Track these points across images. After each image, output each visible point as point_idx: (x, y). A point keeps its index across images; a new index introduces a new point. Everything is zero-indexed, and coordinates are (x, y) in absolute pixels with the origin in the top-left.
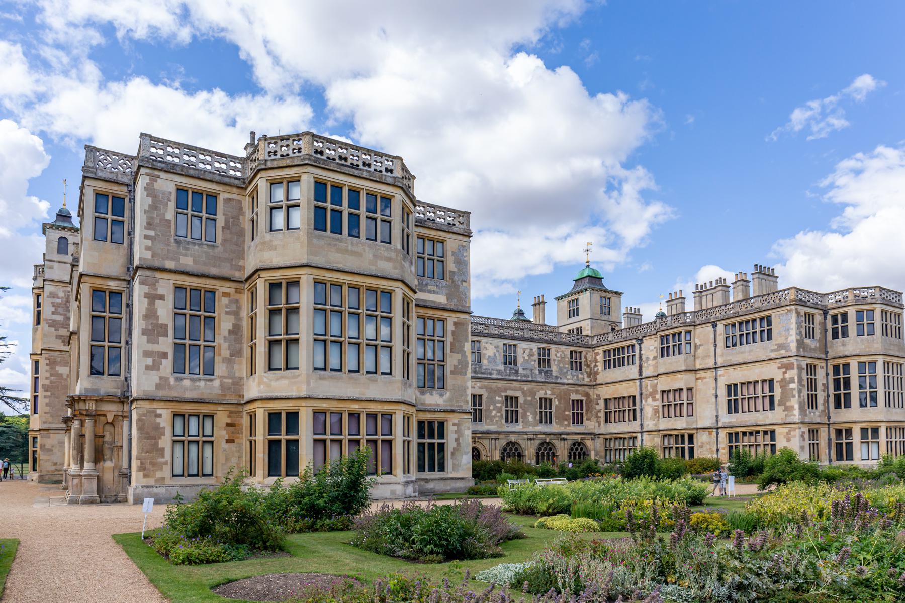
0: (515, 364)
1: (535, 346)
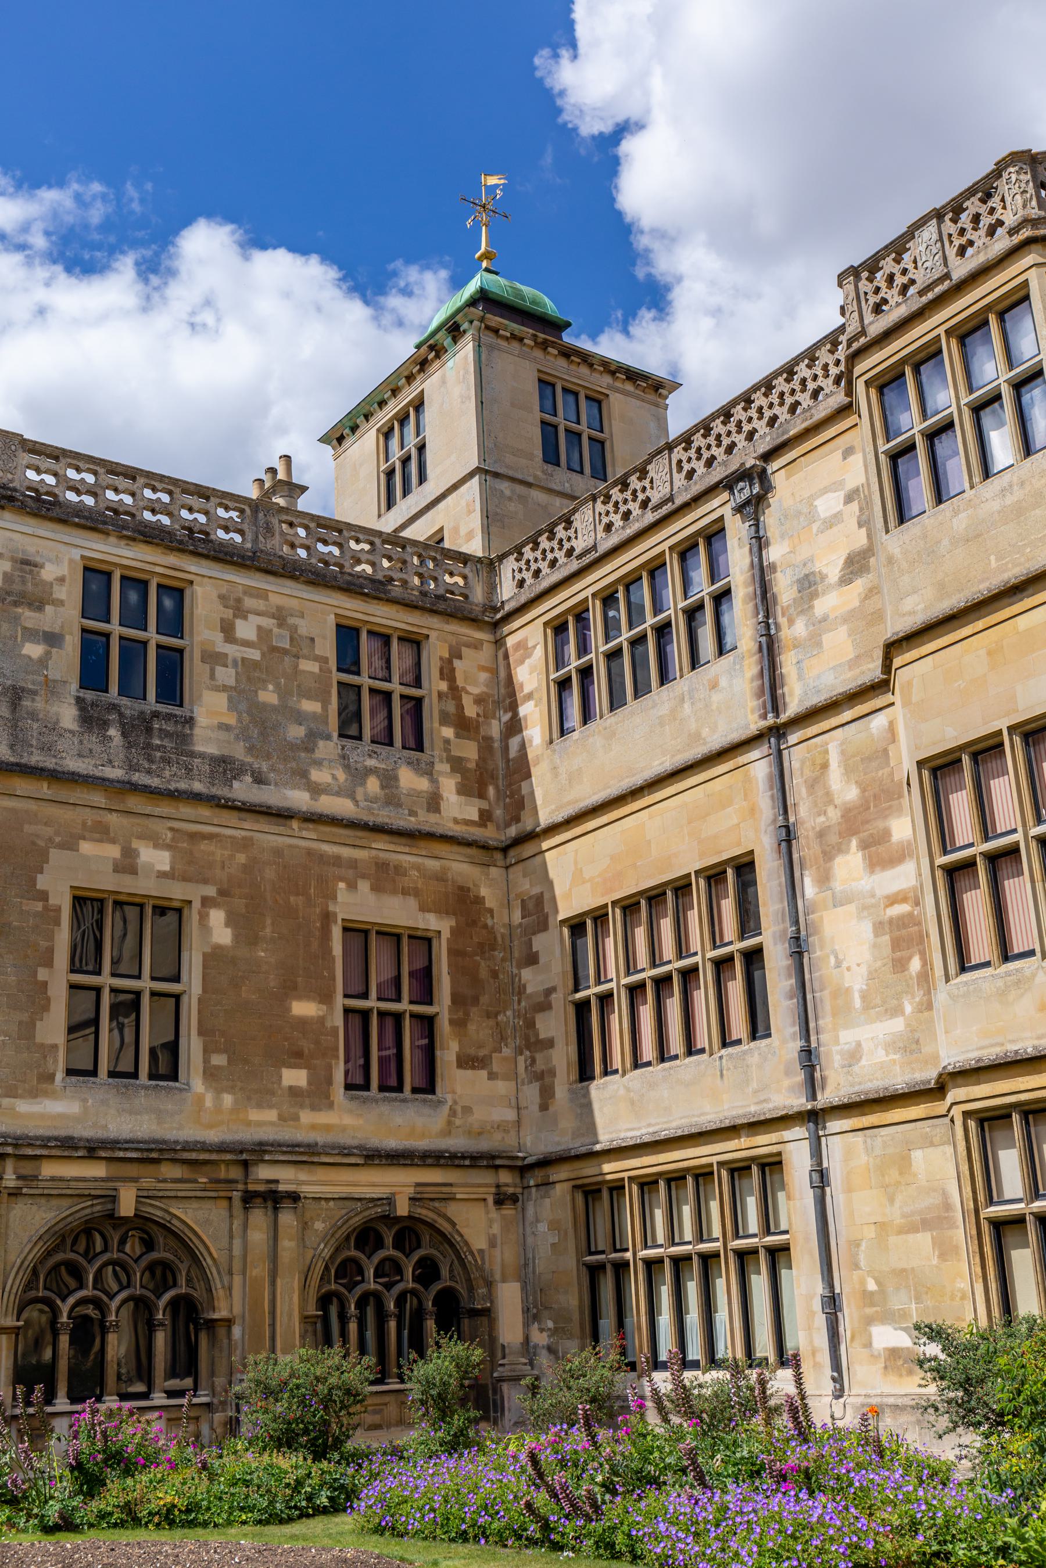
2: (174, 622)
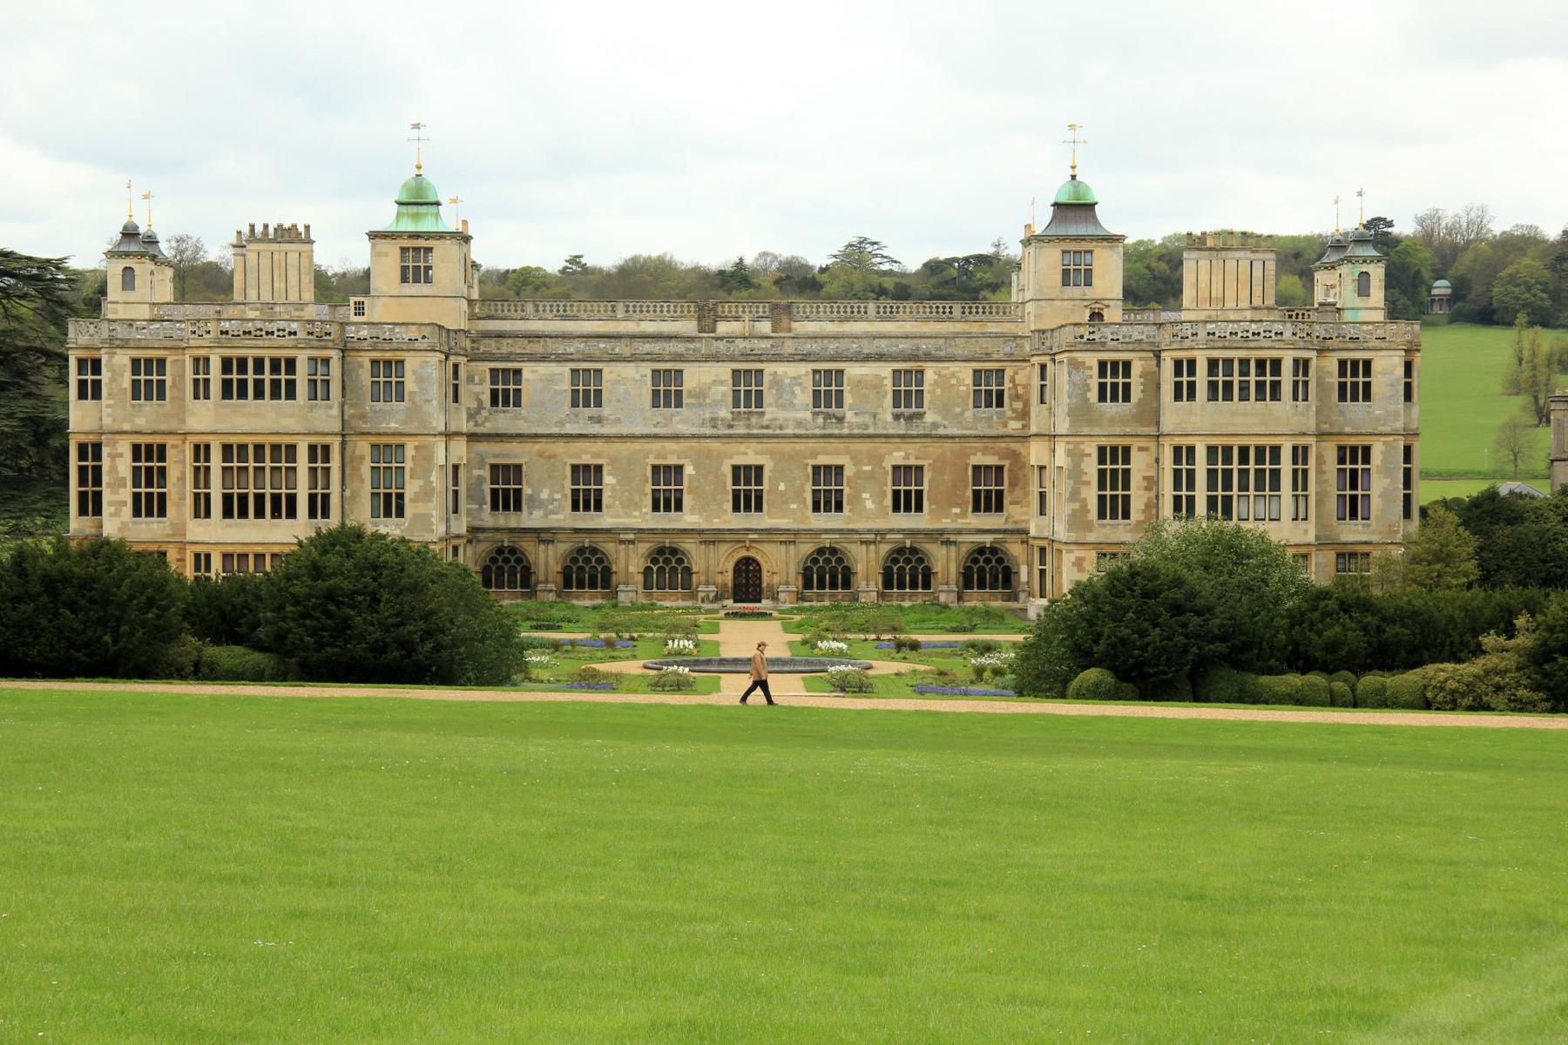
0: (840, 404)
1: (885, 370)
2: (920, 383)
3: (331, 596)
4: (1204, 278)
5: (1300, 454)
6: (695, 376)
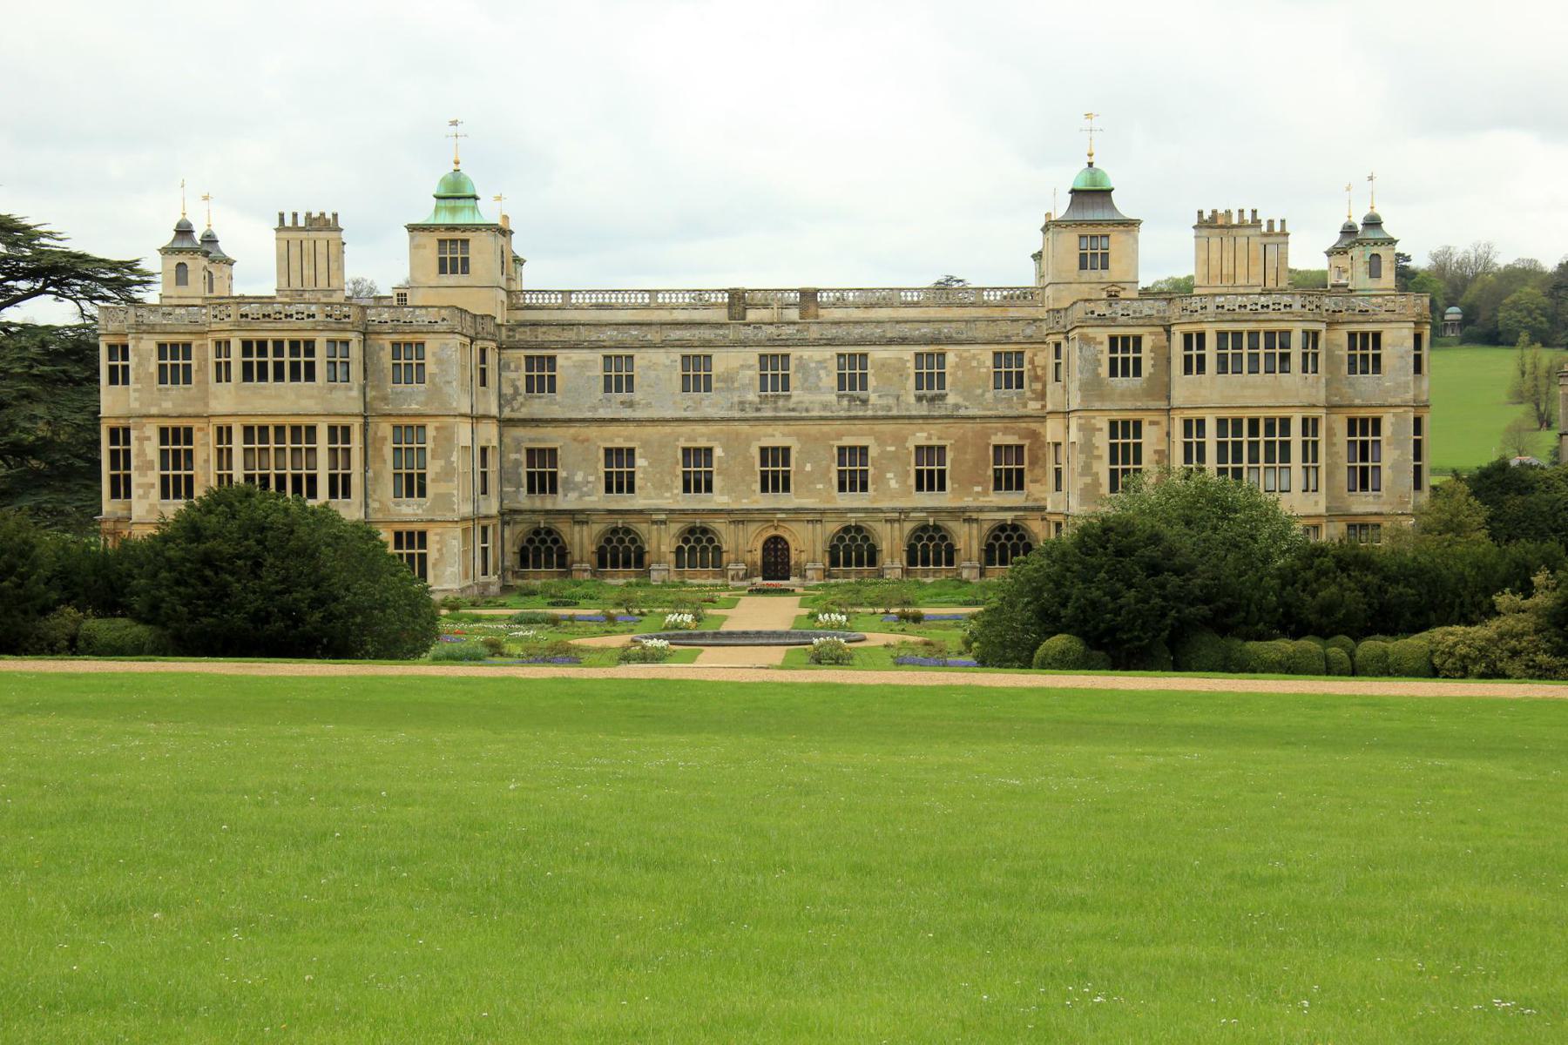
0: (864, 387)
1: (908, 354)
2: (942, 365)
3: (207, 560)
4: (1215, 255)
5: (1310, 426)
6: (723, 360)
